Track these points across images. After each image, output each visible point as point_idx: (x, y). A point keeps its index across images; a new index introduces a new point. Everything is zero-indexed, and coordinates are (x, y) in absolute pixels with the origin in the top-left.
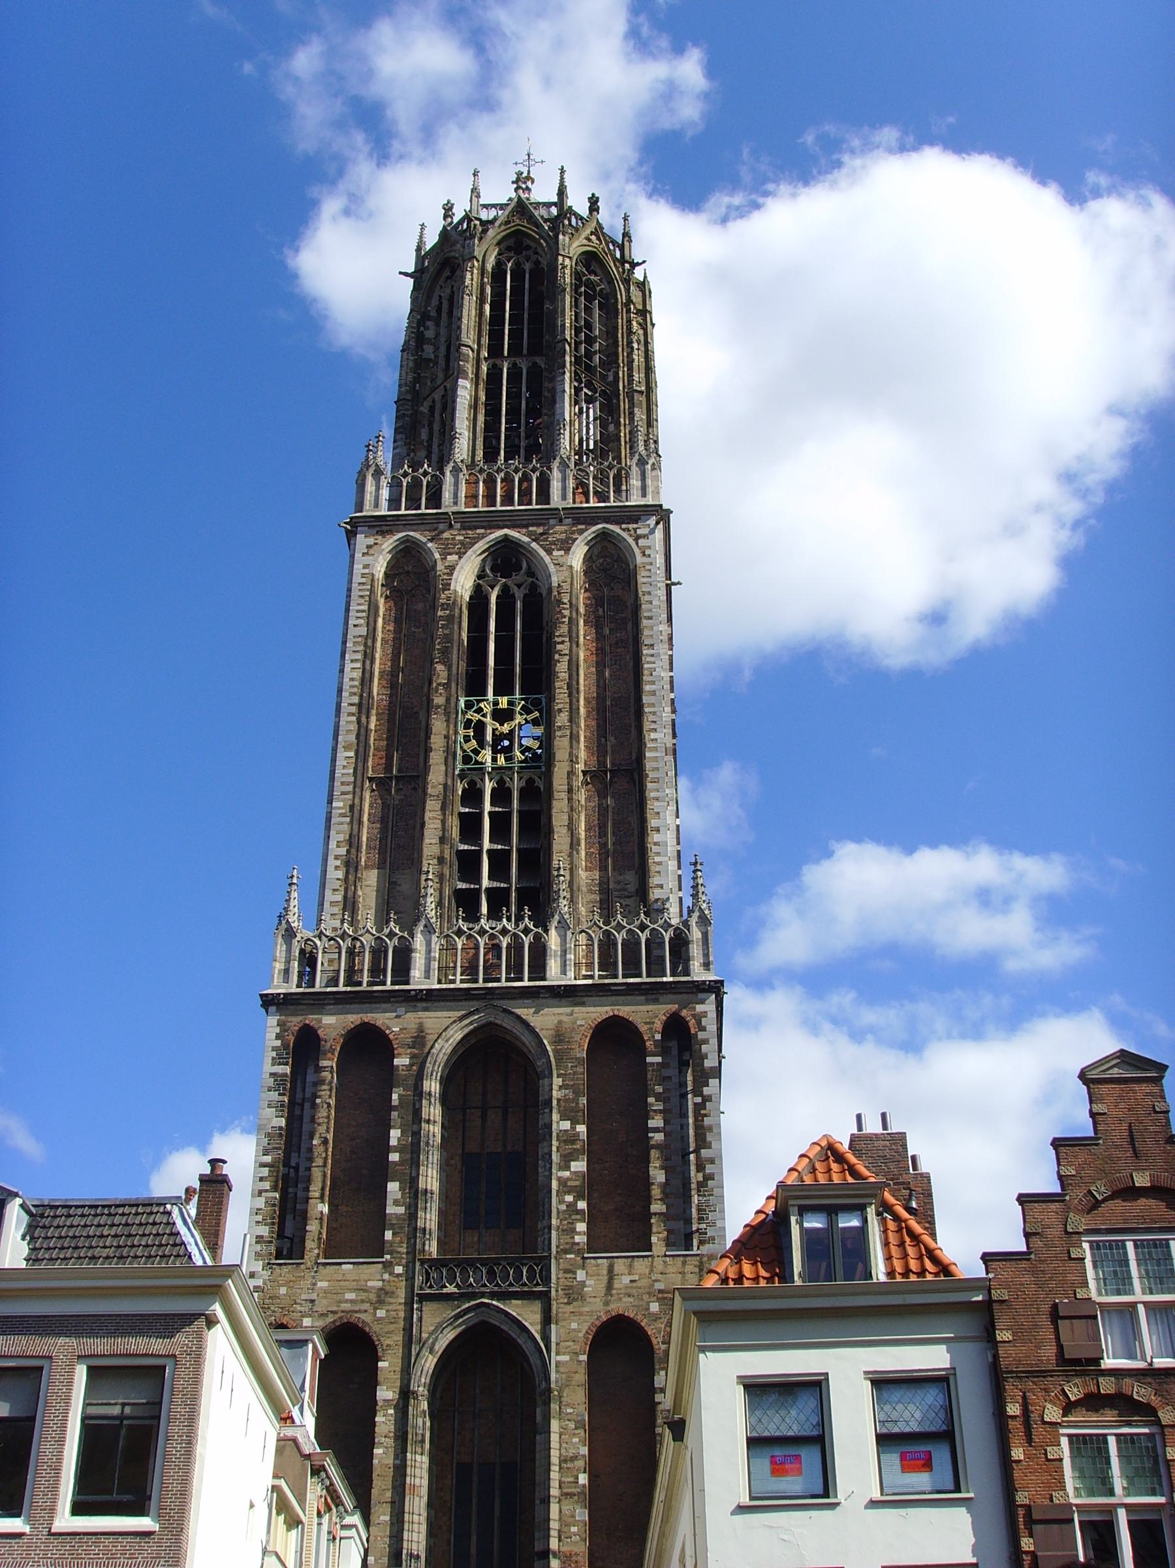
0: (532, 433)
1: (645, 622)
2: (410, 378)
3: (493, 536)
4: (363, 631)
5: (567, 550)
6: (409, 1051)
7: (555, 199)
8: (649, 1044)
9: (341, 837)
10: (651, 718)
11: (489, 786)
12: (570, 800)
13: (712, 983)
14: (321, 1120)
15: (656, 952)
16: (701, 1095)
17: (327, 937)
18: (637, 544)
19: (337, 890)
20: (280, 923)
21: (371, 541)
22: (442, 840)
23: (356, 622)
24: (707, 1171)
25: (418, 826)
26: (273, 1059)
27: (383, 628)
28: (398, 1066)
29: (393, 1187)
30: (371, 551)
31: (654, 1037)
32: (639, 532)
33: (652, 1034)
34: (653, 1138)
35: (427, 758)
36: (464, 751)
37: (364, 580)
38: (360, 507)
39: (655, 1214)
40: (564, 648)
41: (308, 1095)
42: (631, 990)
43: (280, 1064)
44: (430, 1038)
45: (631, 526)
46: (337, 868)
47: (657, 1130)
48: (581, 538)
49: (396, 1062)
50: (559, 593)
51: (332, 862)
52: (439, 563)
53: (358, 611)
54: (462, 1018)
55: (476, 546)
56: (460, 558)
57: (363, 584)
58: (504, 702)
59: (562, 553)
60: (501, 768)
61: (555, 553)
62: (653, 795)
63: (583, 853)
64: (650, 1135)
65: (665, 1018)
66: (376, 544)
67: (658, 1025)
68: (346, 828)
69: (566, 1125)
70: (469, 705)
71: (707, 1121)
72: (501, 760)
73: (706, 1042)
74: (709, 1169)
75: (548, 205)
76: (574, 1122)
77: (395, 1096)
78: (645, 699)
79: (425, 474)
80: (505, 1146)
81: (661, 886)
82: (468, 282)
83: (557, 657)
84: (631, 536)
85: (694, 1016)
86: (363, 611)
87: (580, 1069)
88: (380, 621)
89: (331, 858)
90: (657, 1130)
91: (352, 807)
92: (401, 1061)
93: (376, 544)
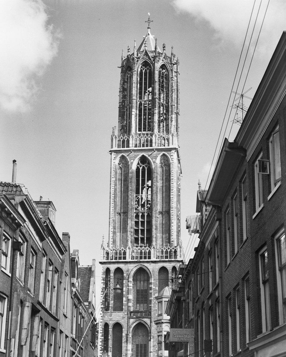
0: (149, 125)
5: (156, 159)
7: (154, 50)
10: (172, 201)
11: (140, 214)
15: (171, 252)
20: (102, 247)
21: (115, 156)
32: (171, 154)
33: (170, 271)
36: (135, 207)
37: (114, 166)
38: (112, 147)
41: (109, 280)
45: (169, 153)
51: (111, 233)
52: (130, 162)
54: (136, 267)
56: (134, 161)
61: (154, 160)
69: (154, 287)
70: (136, 196)
72: (143, 210)
75: (152, 52)
76: (156, 287)
79: (126, 138)
80: (144, 288)
82: (134, 79)
83: (154, 186)
89: (110, 231)
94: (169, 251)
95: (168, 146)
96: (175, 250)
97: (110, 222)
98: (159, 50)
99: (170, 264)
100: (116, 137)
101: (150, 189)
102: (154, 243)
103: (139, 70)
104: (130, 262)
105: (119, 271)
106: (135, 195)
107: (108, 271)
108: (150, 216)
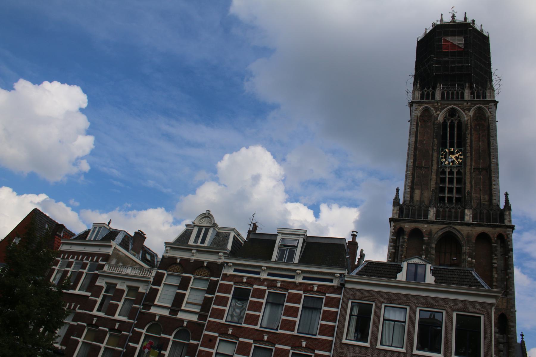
1: (491, 131)
3: (449, 107)
5: (469, 111)
6: (428, 236)
8: (493, 241)
9: (409, 181)
11: (448, 170)
12: (470, 175)
13: (512, 226)
14: (404, 251)
16: (508, 255)
17: (406, 205)
18: (489, 110)
19: (408, 194)
21: (417, 107)
22: (436, 183)
23: (413, 127)
24: (509, 276)
25: (430, 180)
26: (392, 235)
27: (420, 129)
28: (424, 240)
30: (417, 110)
31: (494, 239)
32: (489, 107)
33: (494, 238)
34: (494, 265)
35: (432, 162)
36: (442, 161)
37: (415, 117)
39: (494, 285)
40: (469, 136)
42: (488, 226)
43: (394, 236)
45: (487, 106)
46: (408, 188)
47: (495, 263)
48: (473, 108)
49: (424, 238)
50: (467, 122)
52: (435, 113)
53: (414, 125)
55: (445, 109)
56: (440, 112)
57: (415, 118)
58: (452, 149)
59: (468, 112)
60: (451, 166)
61: (466, 112)
62: (493, 175)
63: (473, 189)
64: (493, 264)
65: (497, 234)
66: (418, 108)
67: (496, 236)
68: (411, 179)
69: (470, 259)
70: (442, 150)
71: (509, 262)
73: (509, 241)
74: (510, 275)
76: (472, 259)
77: (424, 247)
78: (491, 150)
81: (496, 200)
83: (467, 138)
84: (487, 108)
85: (506, 234)
86: (415, 125)
87: (474, 245)
88: (419, 127)
89: (407, 186)
90: (495, 263)
91: (412, 174)
92: (425, 239)
93: (418, 108)
99: (494, 230)
104: (432, 222)
105: (416, 233)
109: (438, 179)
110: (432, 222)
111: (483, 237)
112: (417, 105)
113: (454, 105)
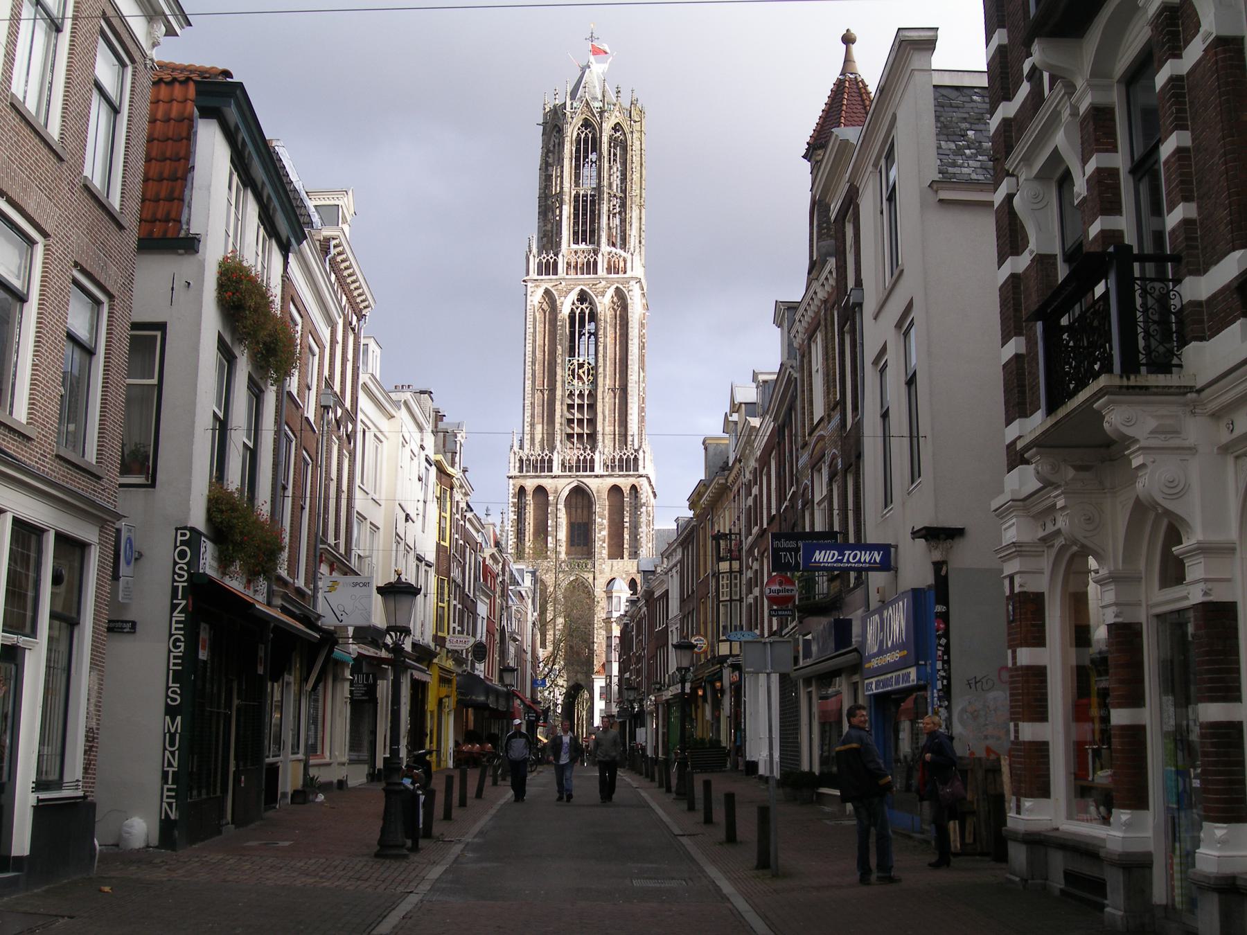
2: (544, 184)
4: (532, 330)
8: (625, 494)
11: (577, 392)
21: (532, 290)
22: (561, 416)
29: (550, 539)
33: (626, 491)
38: (528, 274)
42: (620, 476)
44: (559, 491)
51: (526, 424)
61: (600, 297)
67: (628, 488)
68: (530, 411)
69: (600, 520)
70: (570, 361)
72: (580, 384)
78: (629, 362)
92: (551, 498)
94: (625, 457)
95: (625, 273)
96: (636, 456)
97: (524, 407)
98: (612, 96)
100: (534, 256)
101: (592, 337)
102: (600, 445)
103: (575, 134)
104: (559, 477)
105: (540, 490)
106: (567, 359)
107: (522, 491)
108: (593, 395)
109: (565, 408)
110: (559, 477)
111: (616, 490)
112: (533, 285)
113: (584, 285)
